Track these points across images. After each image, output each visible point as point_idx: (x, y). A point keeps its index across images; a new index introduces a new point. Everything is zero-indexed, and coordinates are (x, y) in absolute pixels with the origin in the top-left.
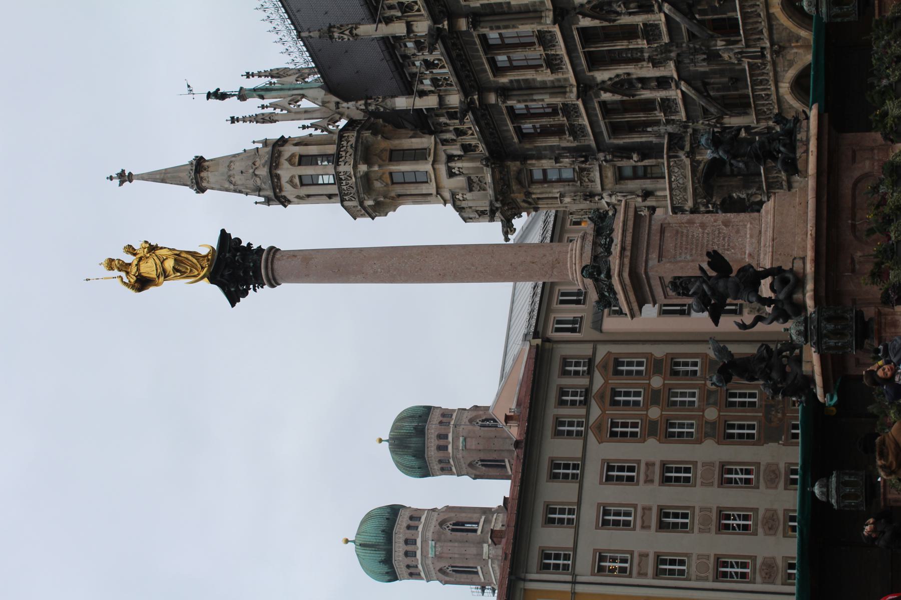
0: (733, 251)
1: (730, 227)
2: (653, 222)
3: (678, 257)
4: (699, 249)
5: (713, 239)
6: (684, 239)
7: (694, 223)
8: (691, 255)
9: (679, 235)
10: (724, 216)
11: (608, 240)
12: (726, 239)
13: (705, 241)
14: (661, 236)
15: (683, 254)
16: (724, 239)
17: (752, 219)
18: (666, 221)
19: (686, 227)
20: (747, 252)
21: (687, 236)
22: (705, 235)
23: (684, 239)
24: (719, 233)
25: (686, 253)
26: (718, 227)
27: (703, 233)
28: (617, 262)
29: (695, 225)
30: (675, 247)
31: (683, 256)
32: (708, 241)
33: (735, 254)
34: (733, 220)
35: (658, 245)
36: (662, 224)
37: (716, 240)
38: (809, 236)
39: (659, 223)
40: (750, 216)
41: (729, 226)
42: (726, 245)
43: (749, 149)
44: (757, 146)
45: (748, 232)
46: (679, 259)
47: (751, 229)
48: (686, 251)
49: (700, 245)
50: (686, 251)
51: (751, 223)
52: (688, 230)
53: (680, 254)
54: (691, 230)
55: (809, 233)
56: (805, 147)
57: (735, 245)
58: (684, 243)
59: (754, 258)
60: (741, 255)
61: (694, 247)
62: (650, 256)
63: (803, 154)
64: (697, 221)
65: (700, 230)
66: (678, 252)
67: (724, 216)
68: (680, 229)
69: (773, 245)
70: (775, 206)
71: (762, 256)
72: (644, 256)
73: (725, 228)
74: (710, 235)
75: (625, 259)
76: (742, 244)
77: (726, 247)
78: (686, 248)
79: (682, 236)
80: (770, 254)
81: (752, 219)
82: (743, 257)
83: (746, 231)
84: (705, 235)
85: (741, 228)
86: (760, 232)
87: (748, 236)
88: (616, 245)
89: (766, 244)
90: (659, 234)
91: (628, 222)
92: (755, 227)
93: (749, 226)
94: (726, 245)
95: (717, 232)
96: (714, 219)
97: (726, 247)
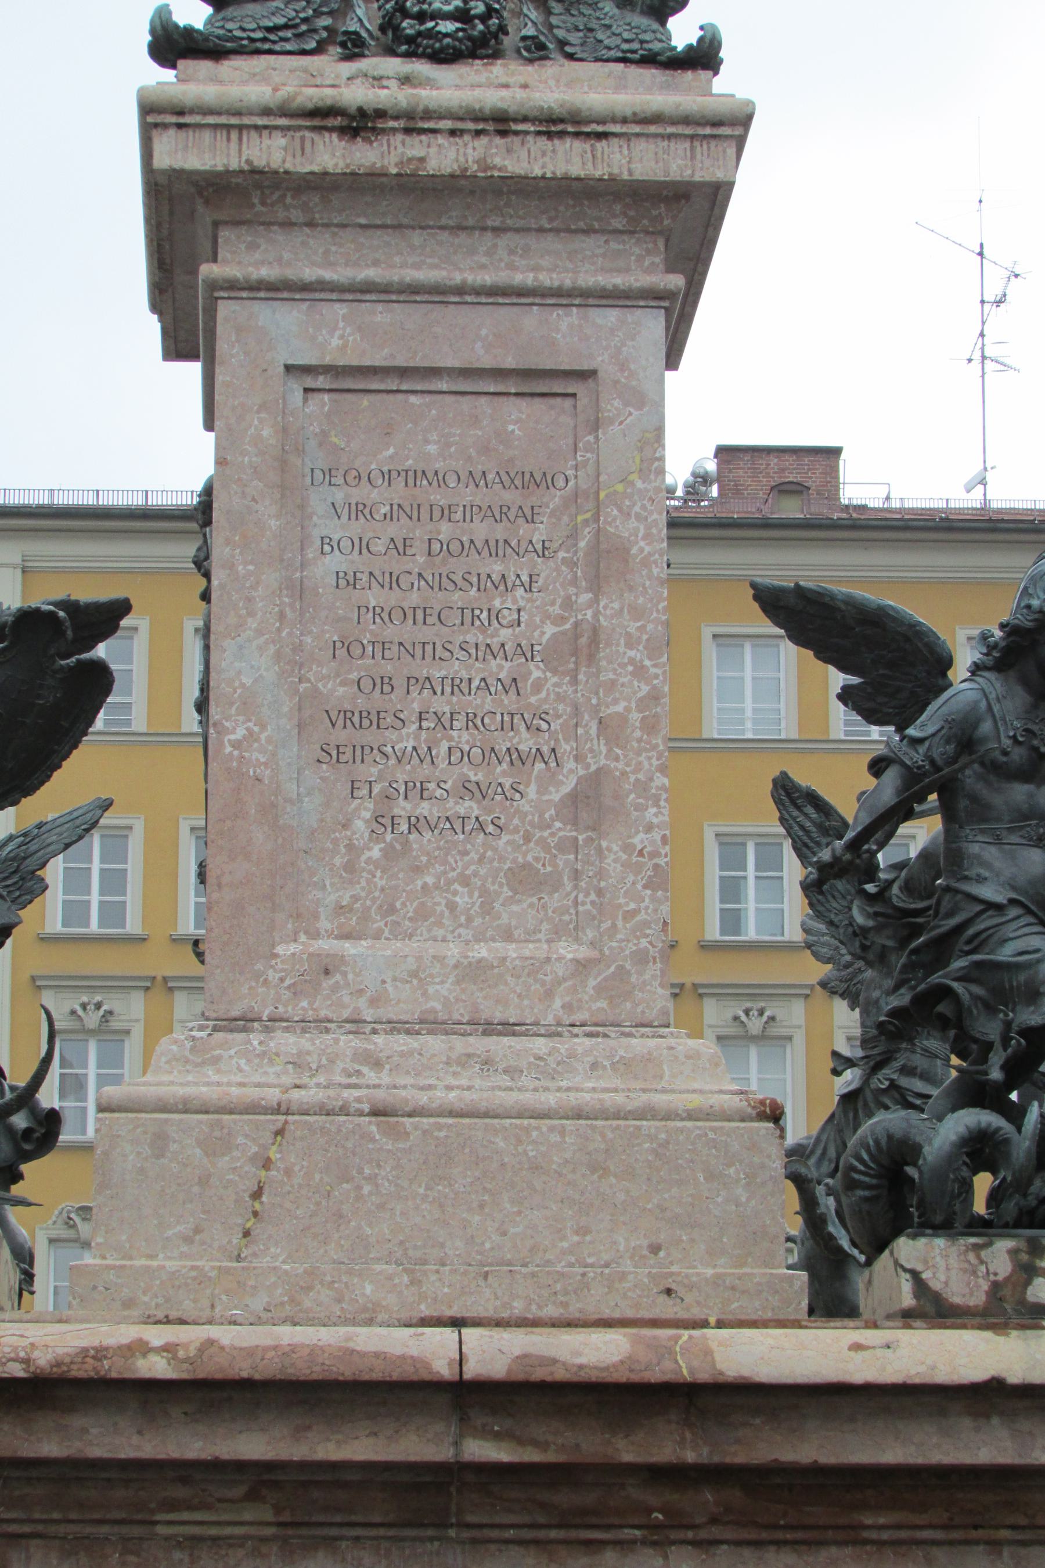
0: (376, 852)
1: (562, 830)
2: (610, 317)
3: (339, 496)
4: (391, 632)
5: (471, 721)
6: (481, 530)
7: (596, 585)
8: (349, 581)
9: (509, 497)
10: (643, 787)
11: (447, 27)
12: (470, 807)
13: (456, 668)
14: (499, 373)
15: (356, 528)
16: (467, 789)
17: (622, 973)
18: (612, 405)
19: (574, 535)
20: (349, 948)
21: (494, 549)
22: (503, 669)
23: (481, 530)
24: (519, 759)
25: (363, 546)
26: (565, 747)
27: (527, 653)
28: (258, 93)
29: (585, 597)
30: (414, 476)
31: (335, 529)
32: (456, 685)
33: (350, 867)
34: (612, 845)
35: (418, 362)
36: (587, 375)
37: (463, 738)
38: (126, 1333)
39: (600, 360)
40: (641, 958)
41: (575, 822)
42: (424, 808)
43: (989, 892)
44: (1006, 954)
45: (512, 951)
46: (318, 501)
47: (536, 967)
48: (379, 547)
49: (426, 633)
50: (379, 547)
51: (582, 967)
52: (544, 552)
53: (360, 510)
54: (544, 569)
55: (157, 1336)
56: (978, 1299)
57: (418, 870)
58: (445, 530)
59: (296, 991)
60: (340, 909)
61: (414, 598)
62: (341, 309)
63: (906, 1286)
64: (610, 605)
65: (550, 630)
66: (362, 493)
67: (643, 787)
68: (555, 499)
69: (344, 1110)
70: (669, 1115)
71: (286, 1042)
72: (328, 275)
73: (556, 795)
74: (509, 701)
75: (279, 141)
76: (423, 914)
77: (402, 808)
78: (402, 547)
79: (500, 514)
80: (273, 1095)
81: (622, 973)
82: (324, 924)
83: (530, 936)
84: (503, 669)
85: (555, 901)
86: (508, 1028)
87: (482, 952)
88: (406, 80)
89: (377, 1065)
90: (510, 362)
91: (578, 145)
92: (549, 994)
93: (567, 950)
94: (424, 808)
95: (526, 743)
96: (623, 719)
97: (402, 808)
